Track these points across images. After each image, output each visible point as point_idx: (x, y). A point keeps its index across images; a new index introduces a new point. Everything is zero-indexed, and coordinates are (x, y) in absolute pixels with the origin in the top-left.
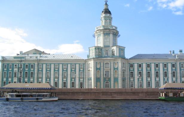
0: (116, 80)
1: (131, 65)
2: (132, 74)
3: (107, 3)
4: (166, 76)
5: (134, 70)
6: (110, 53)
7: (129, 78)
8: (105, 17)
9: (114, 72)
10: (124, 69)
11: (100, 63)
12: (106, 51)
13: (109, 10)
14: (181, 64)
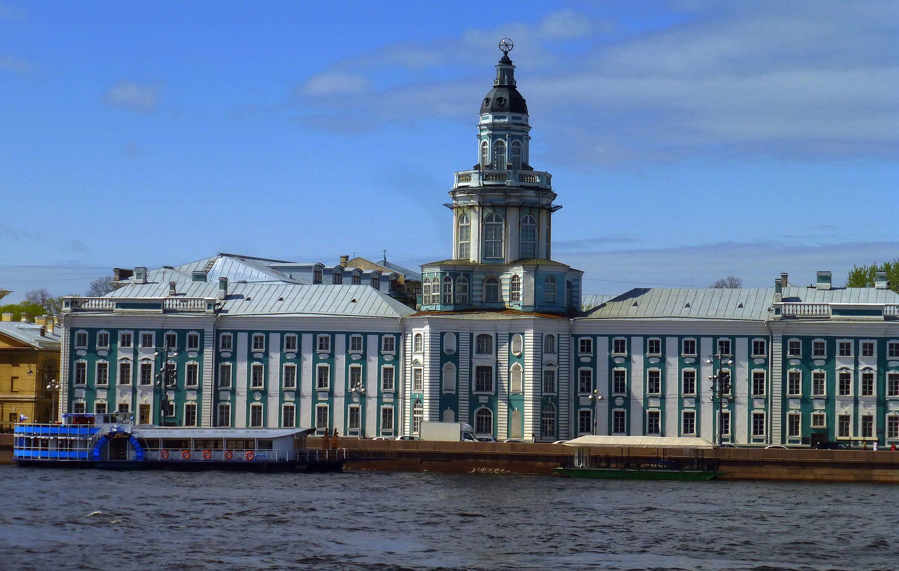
1: (583, 342)
5: (593, 363)
7: (576, 394)
8: (493, 130)
9: (509, 372)
11: (457, 335)
12: (488, 282)
14: (791, 343)
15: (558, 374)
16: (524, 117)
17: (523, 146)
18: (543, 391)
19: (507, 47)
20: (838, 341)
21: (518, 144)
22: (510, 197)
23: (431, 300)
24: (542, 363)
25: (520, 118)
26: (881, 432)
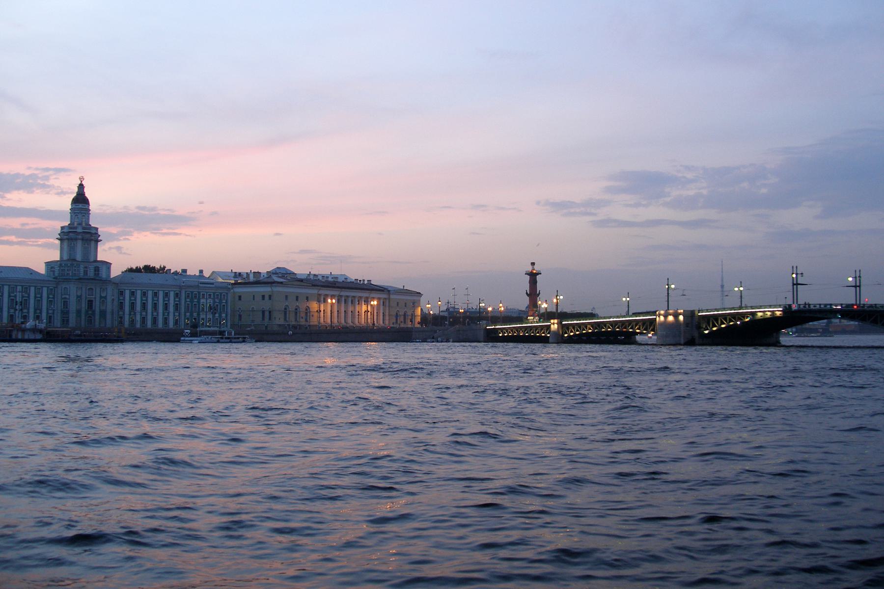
0: (103, 314)
2: (121, 306)
3: (83, 183)
4: (167, 310)
6: (90, 272)
11: (82, 288)
13: (86, 195)
19: (82, 179)
20: (201, 293)
22: (92, 236)
23: (66, 274)
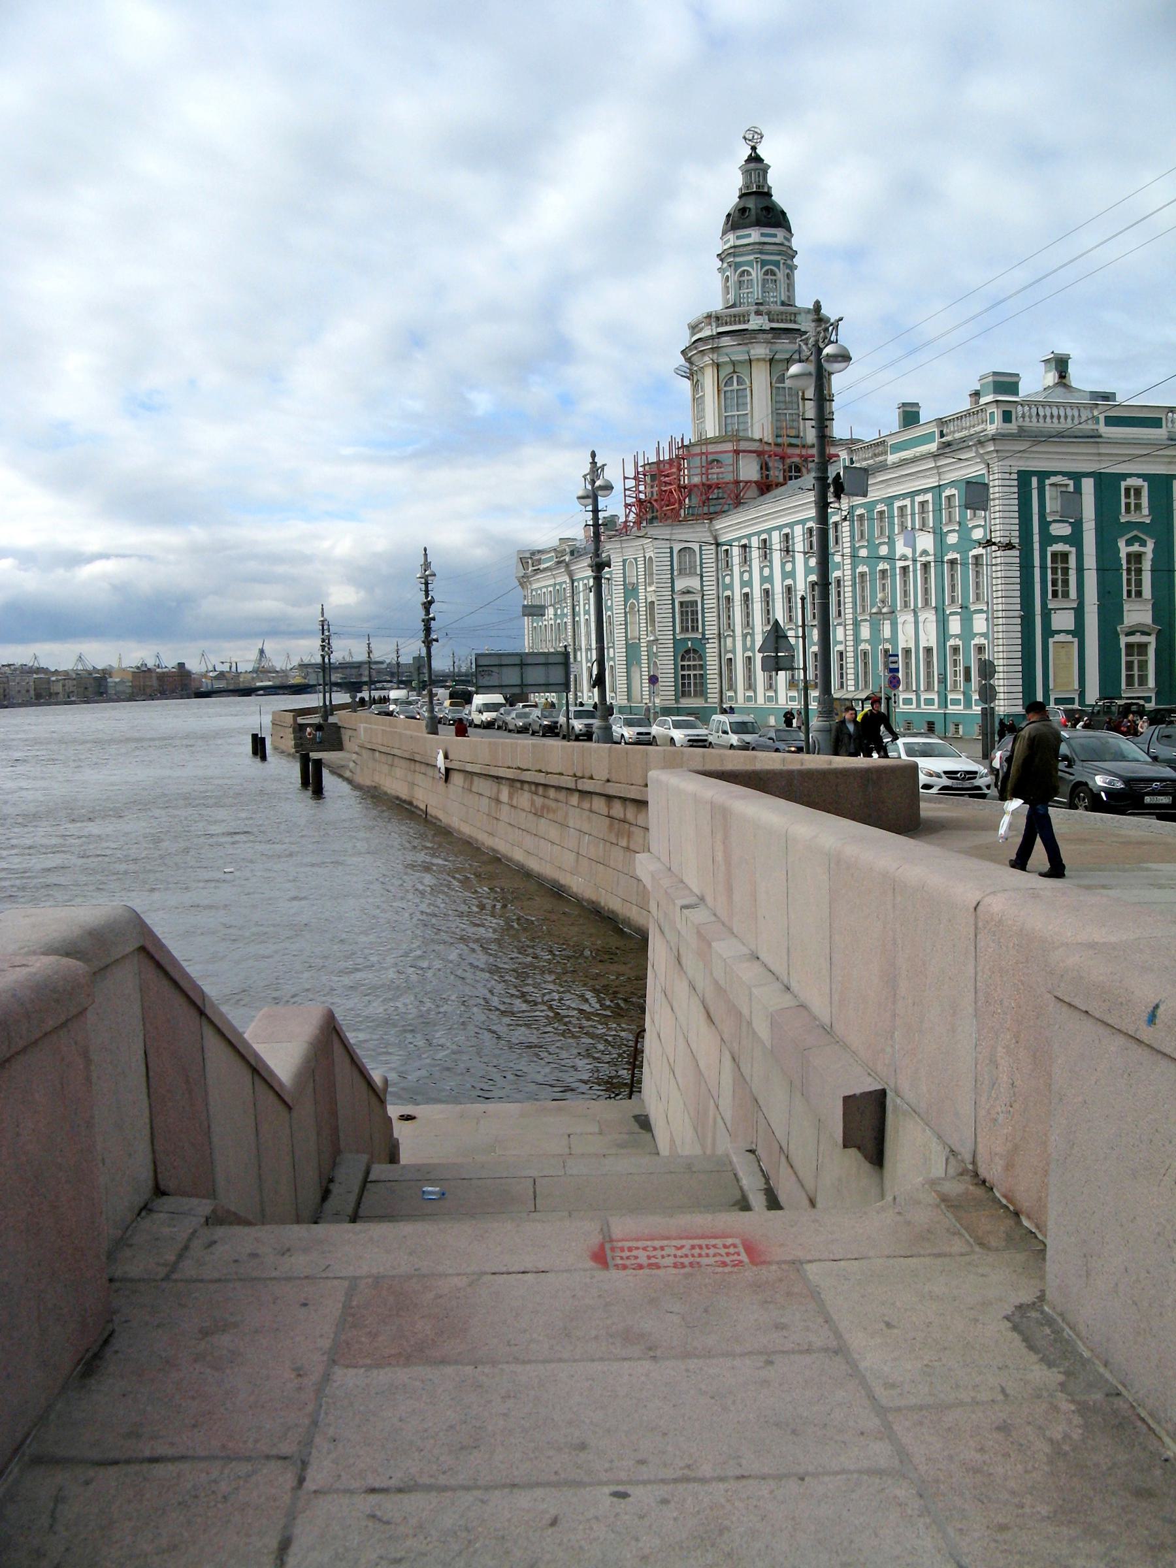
10: (694, 583)
15: (703, 604)
16: (780, 233)
17: (781, 275)
18: (678, 632)
19: (753, 138)
21: (749, 273)
24: (673, 591)
25: (749, 236)
26: (943, 680)
